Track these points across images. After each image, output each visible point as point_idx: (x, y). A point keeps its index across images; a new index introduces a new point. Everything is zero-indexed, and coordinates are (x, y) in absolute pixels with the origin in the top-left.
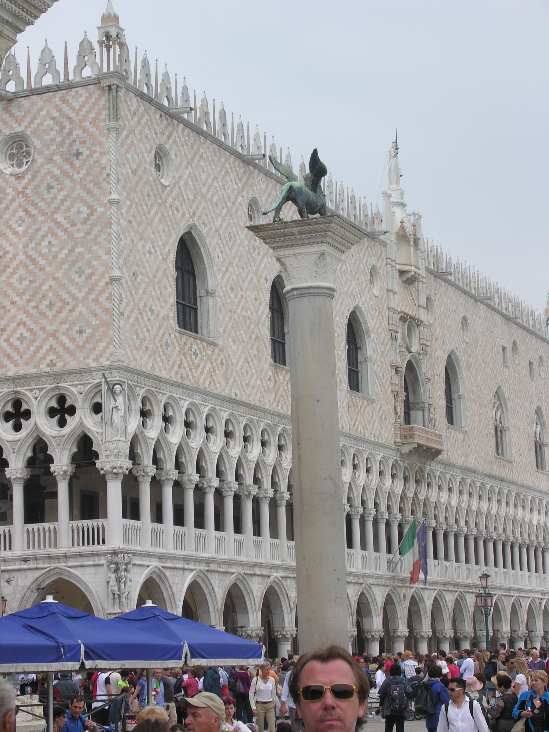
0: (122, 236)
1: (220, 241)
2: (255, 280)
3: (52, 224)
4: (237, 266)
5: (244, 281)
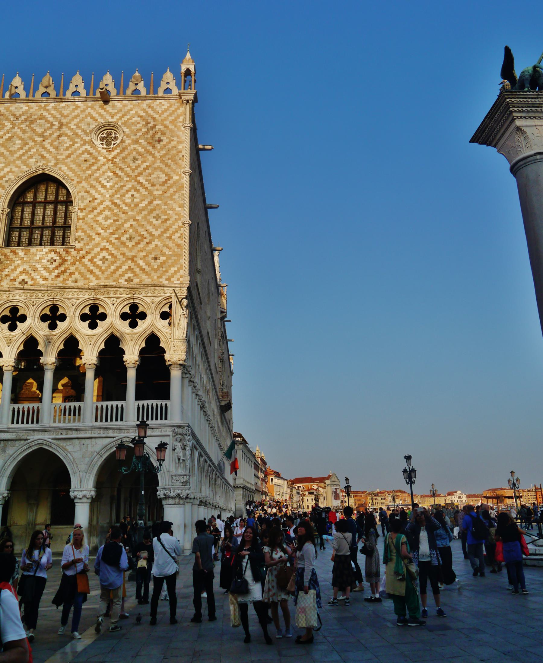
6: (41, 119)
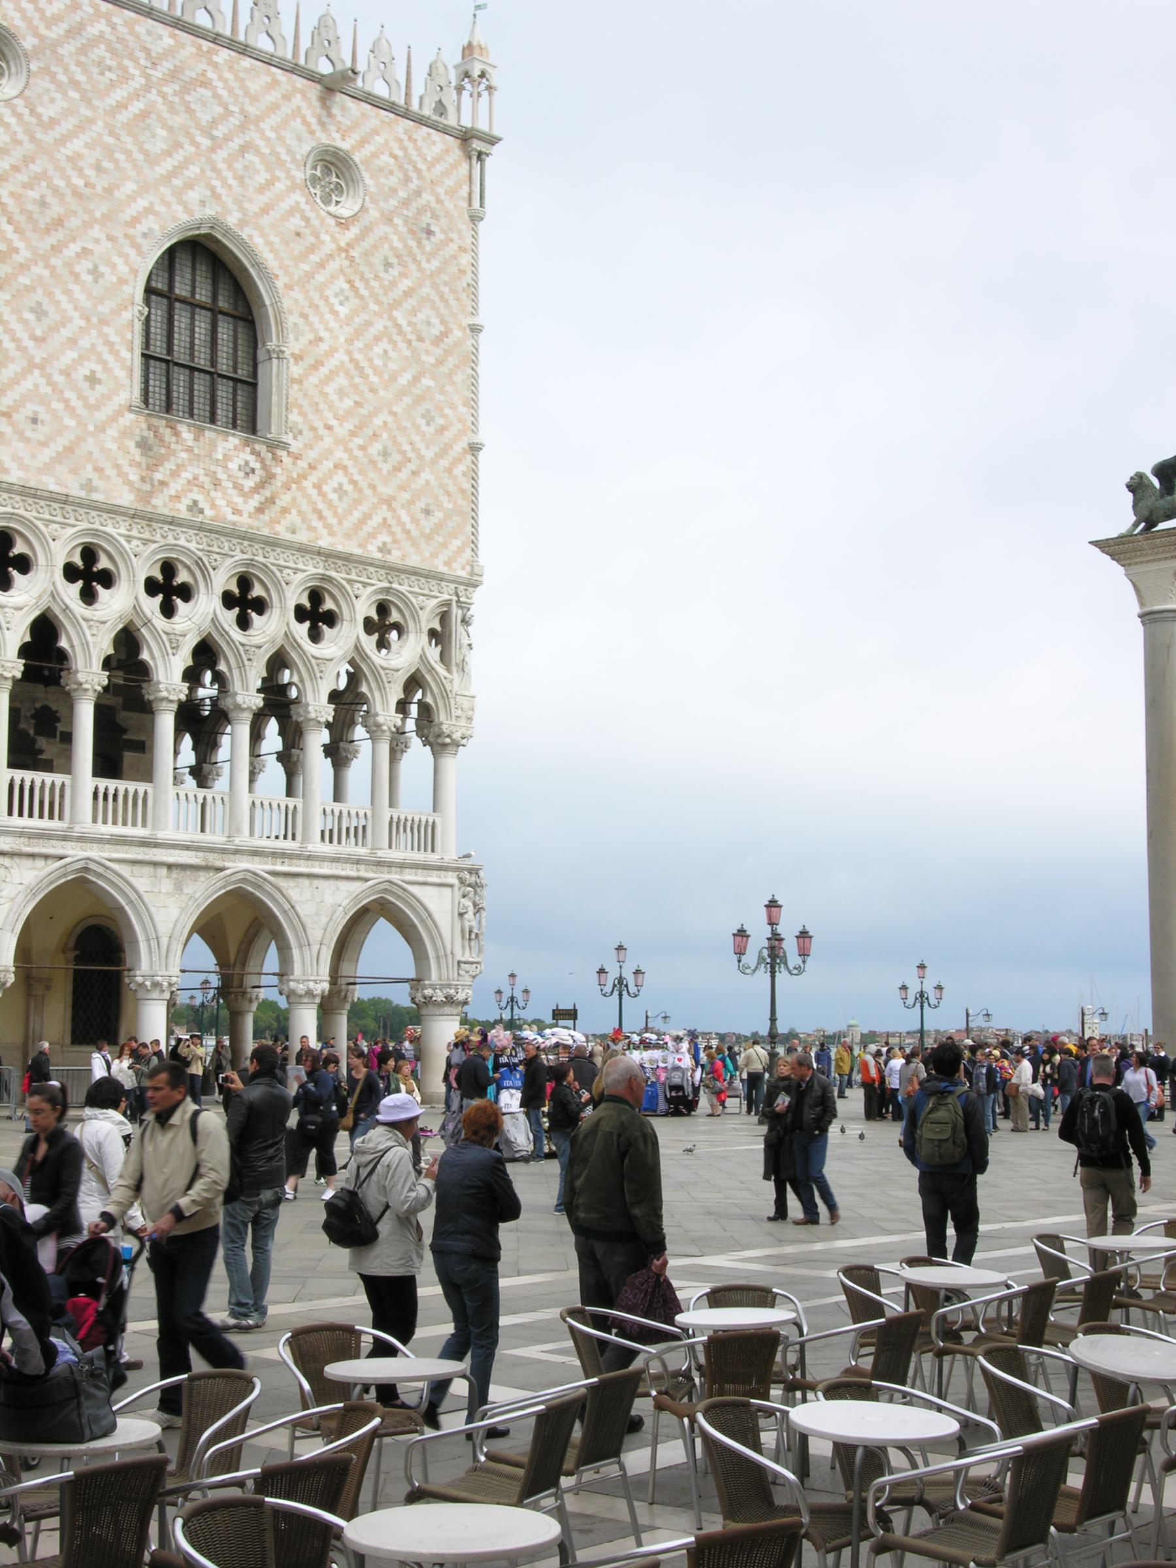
3: (390, 324)
6: (205, 84)
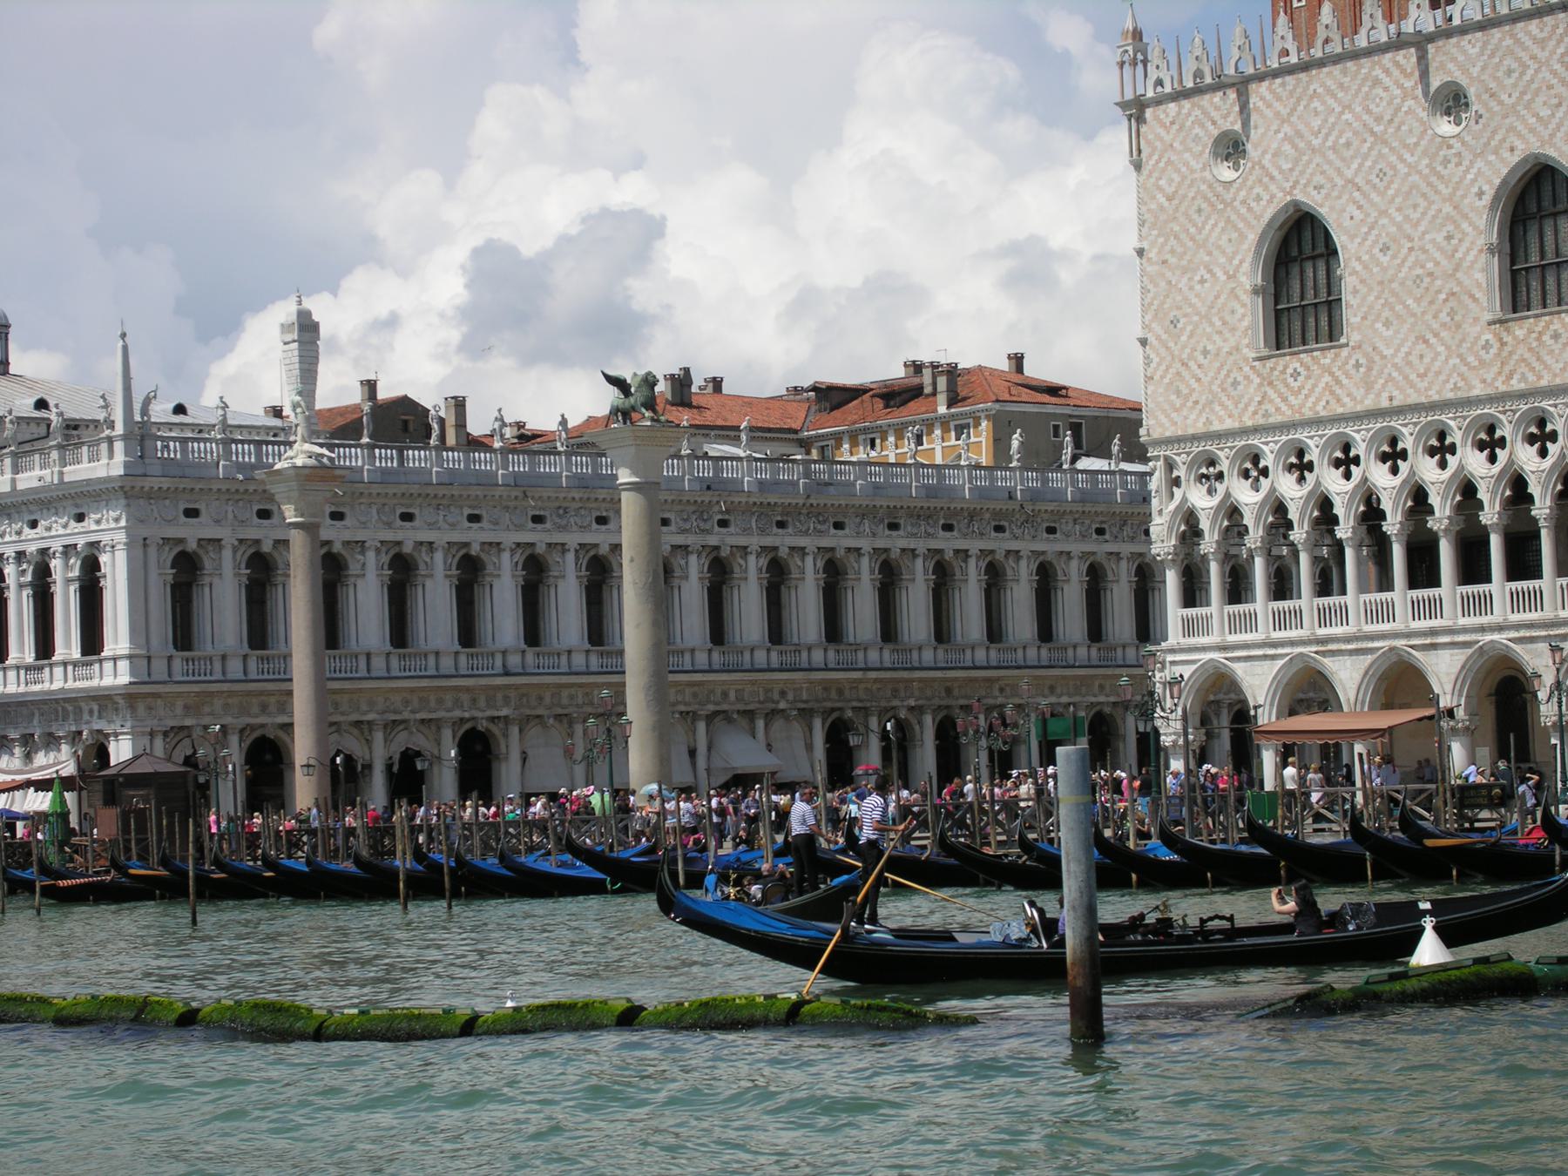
0: (1150, 287)
1: (1356, 194)
2: (1447, 209)
4: (1399, 209)
5: (1416, 225)
